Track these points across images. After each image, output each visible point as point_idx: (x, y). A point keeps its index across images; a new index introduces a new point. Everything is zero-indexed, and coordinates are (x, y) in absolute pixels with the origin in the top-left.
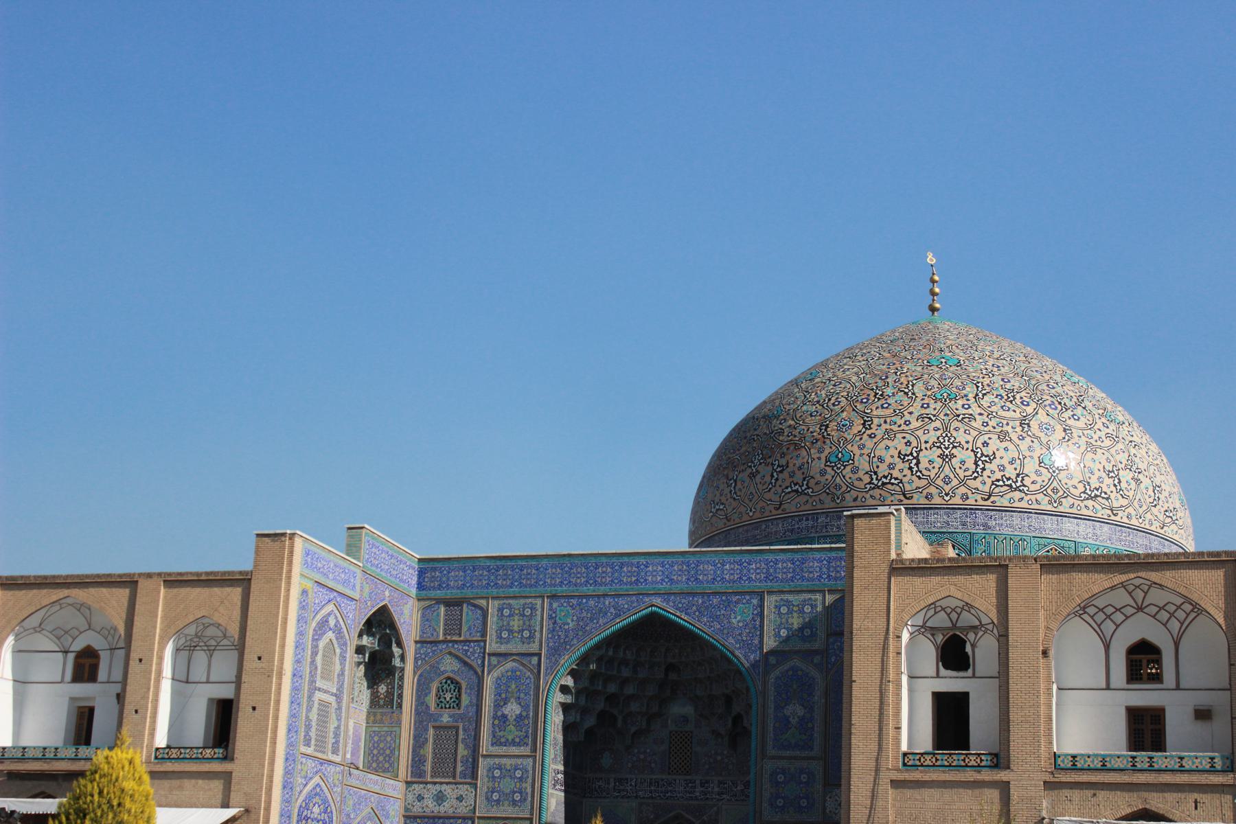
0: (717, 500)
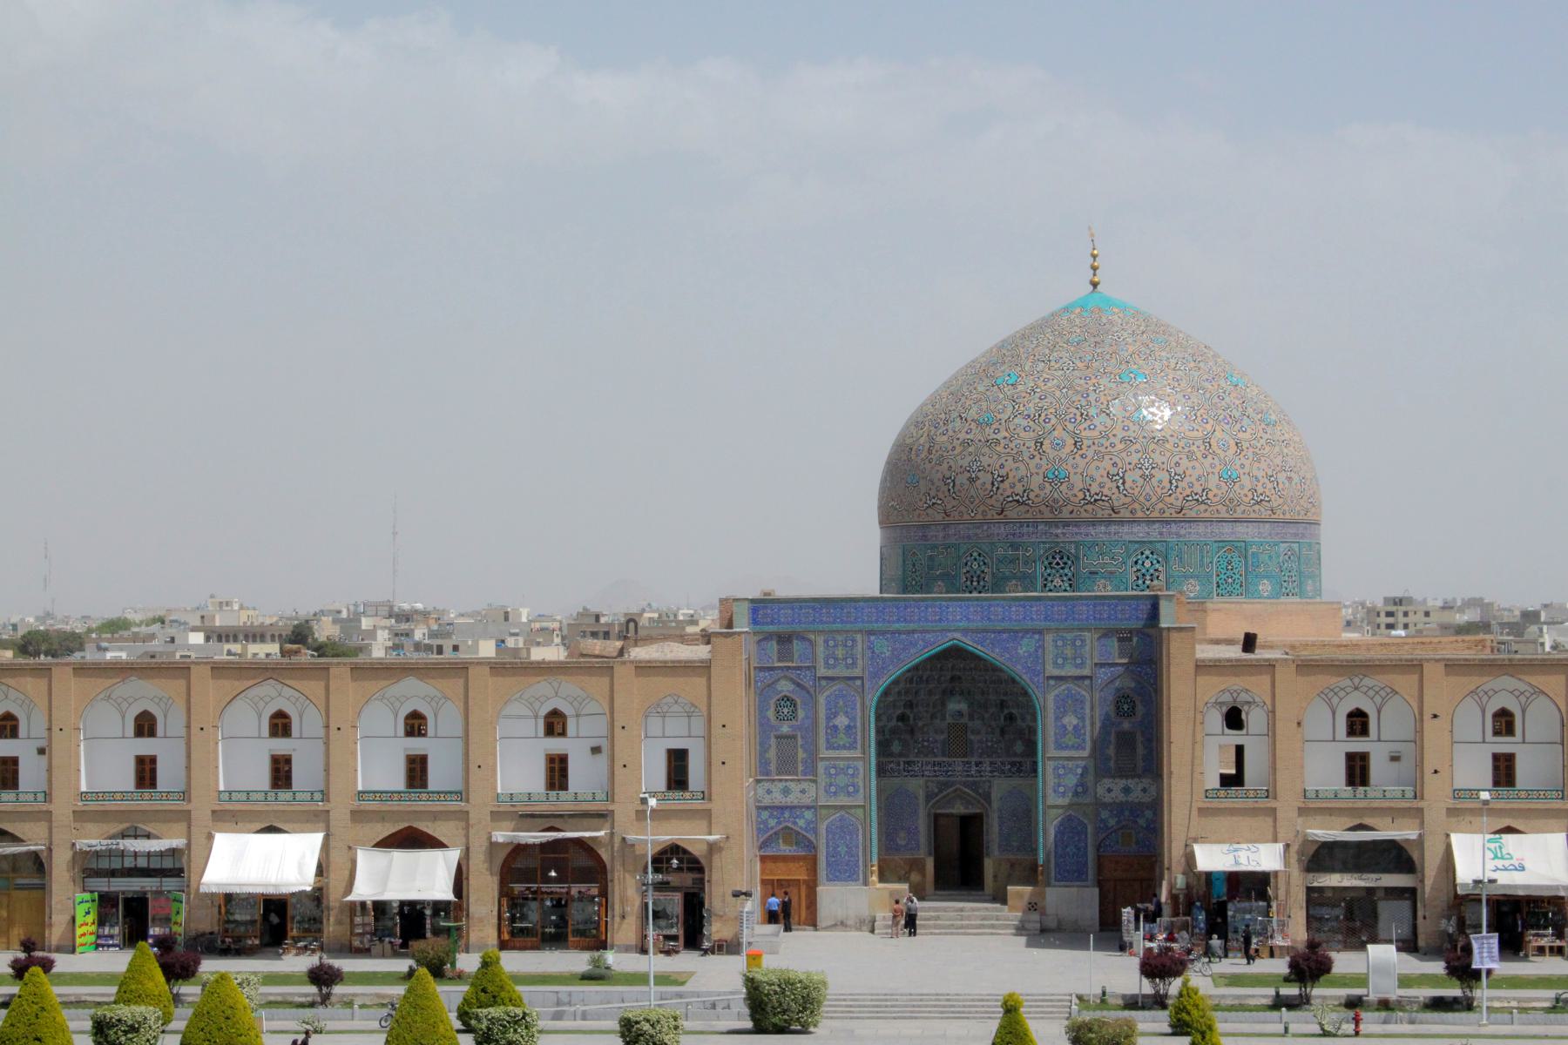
0: (933, 493)
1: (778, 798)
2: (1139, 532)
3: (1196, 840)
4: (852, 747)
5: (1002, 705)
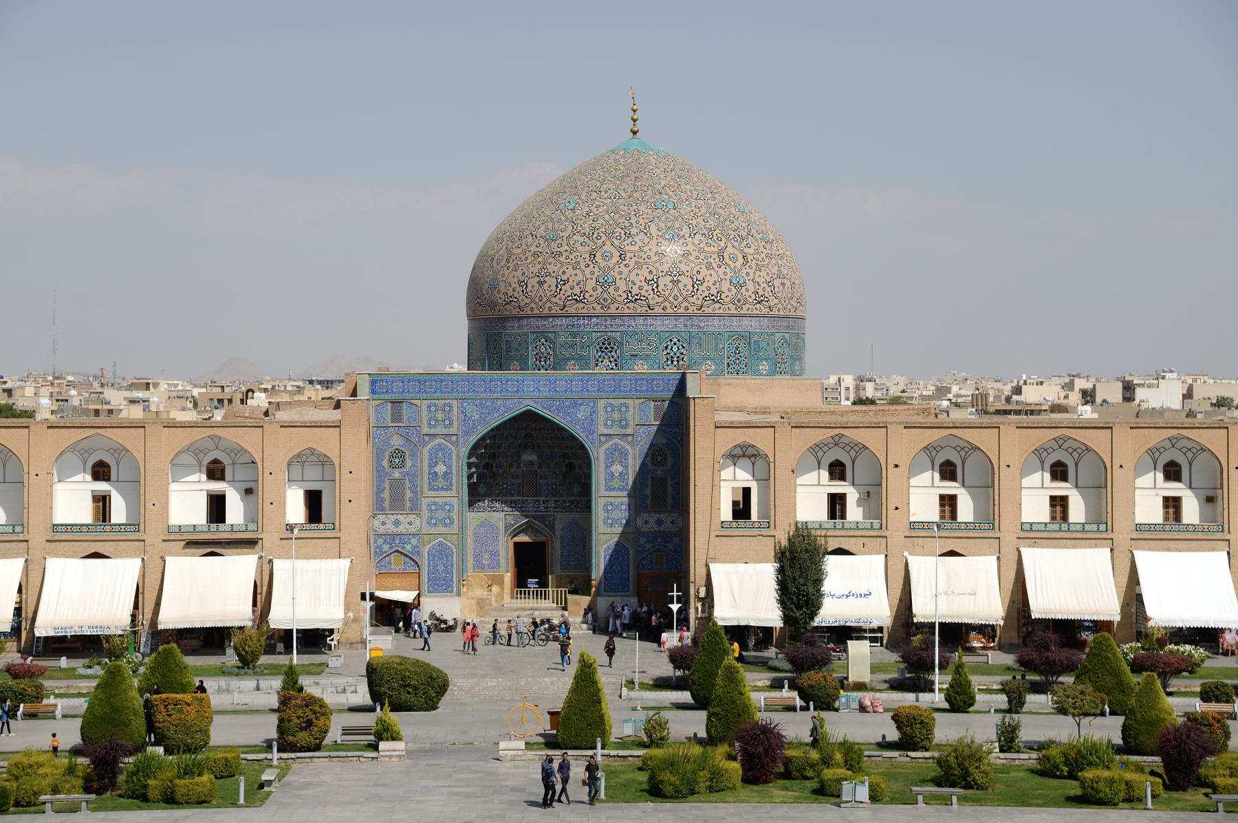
0: (510, 293)
1: (391, 528)
2: (669, 324)
3: (715, 560)
4: (449, 488)
5: (565, 456)
